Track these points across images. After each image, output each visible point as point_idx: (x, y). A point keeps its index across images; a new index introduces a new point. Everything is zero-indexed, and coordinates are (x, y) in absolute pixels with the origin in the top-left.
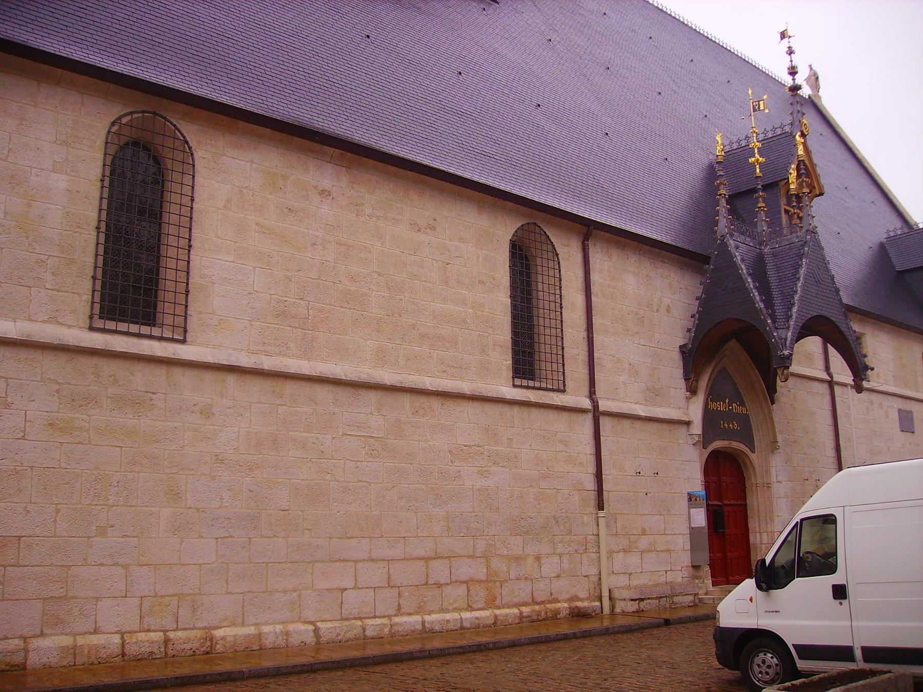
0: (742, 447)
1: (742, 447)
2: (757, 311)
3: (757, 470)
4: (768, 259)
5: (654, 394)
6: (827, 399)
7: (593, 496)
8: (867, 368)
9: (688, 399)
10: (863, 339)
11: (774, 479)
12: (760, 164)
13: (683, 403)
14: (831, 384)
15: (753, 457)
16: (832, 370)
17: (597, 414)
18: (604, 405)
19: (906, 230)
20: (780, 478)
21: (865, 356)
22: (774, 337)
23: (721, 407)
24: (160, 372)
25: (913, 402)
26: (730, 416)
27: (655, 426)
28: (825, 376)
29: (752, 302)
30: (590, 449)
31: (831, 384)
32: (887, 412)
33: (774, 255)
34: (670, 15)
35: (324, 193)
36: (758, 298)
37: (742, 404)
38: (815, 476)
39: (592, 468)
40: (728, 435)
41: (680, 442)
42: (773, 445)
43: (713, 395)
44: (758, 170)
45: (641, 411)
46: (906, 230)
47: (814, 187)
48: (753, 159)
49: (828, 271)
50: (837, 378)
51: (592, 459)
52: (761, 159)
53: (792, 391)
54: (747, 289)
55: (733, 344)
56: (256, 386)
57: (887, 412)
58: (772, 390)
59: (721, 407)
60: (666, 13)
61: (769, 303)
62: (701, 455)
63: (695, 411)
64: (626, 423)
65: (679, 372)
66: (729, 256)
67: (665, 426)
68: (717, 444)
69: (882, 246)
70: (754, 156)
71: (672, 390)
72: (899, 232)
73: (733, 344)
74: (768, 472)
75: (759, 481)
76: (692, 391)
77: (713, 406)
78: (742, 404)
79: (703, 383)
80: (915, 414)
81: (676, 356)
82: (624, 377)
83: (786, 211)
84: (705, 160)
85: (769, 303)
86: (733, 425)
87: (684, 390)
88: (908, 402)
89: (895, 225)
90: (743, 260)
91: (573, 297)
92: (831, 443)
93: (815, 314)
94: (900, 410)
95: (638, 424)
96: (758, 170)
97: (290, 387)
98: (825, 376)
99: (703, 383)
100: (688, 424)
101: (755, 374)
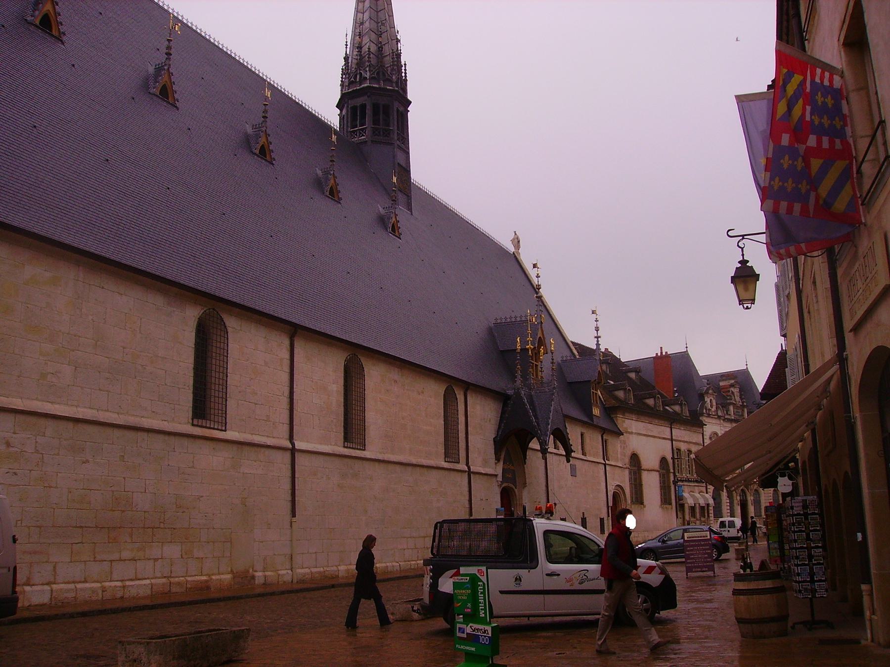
5: (485, 462)
7: (468, 510)
8: (573, 451)
15: (516, 490)
17: (470, 473)
18: (473, 469)
24: (360, 462)
30: (467, 489)
35: (396, 381)
39: (467, 498)
42: (525, 485)
51: (467, 493)
56: (383, 465)
63: (499, 470)
76: (498, 459)
91: (462, 419)
92: (544, 484)
97: (391, 467)
99: (502, 456)
100: (496, 476)
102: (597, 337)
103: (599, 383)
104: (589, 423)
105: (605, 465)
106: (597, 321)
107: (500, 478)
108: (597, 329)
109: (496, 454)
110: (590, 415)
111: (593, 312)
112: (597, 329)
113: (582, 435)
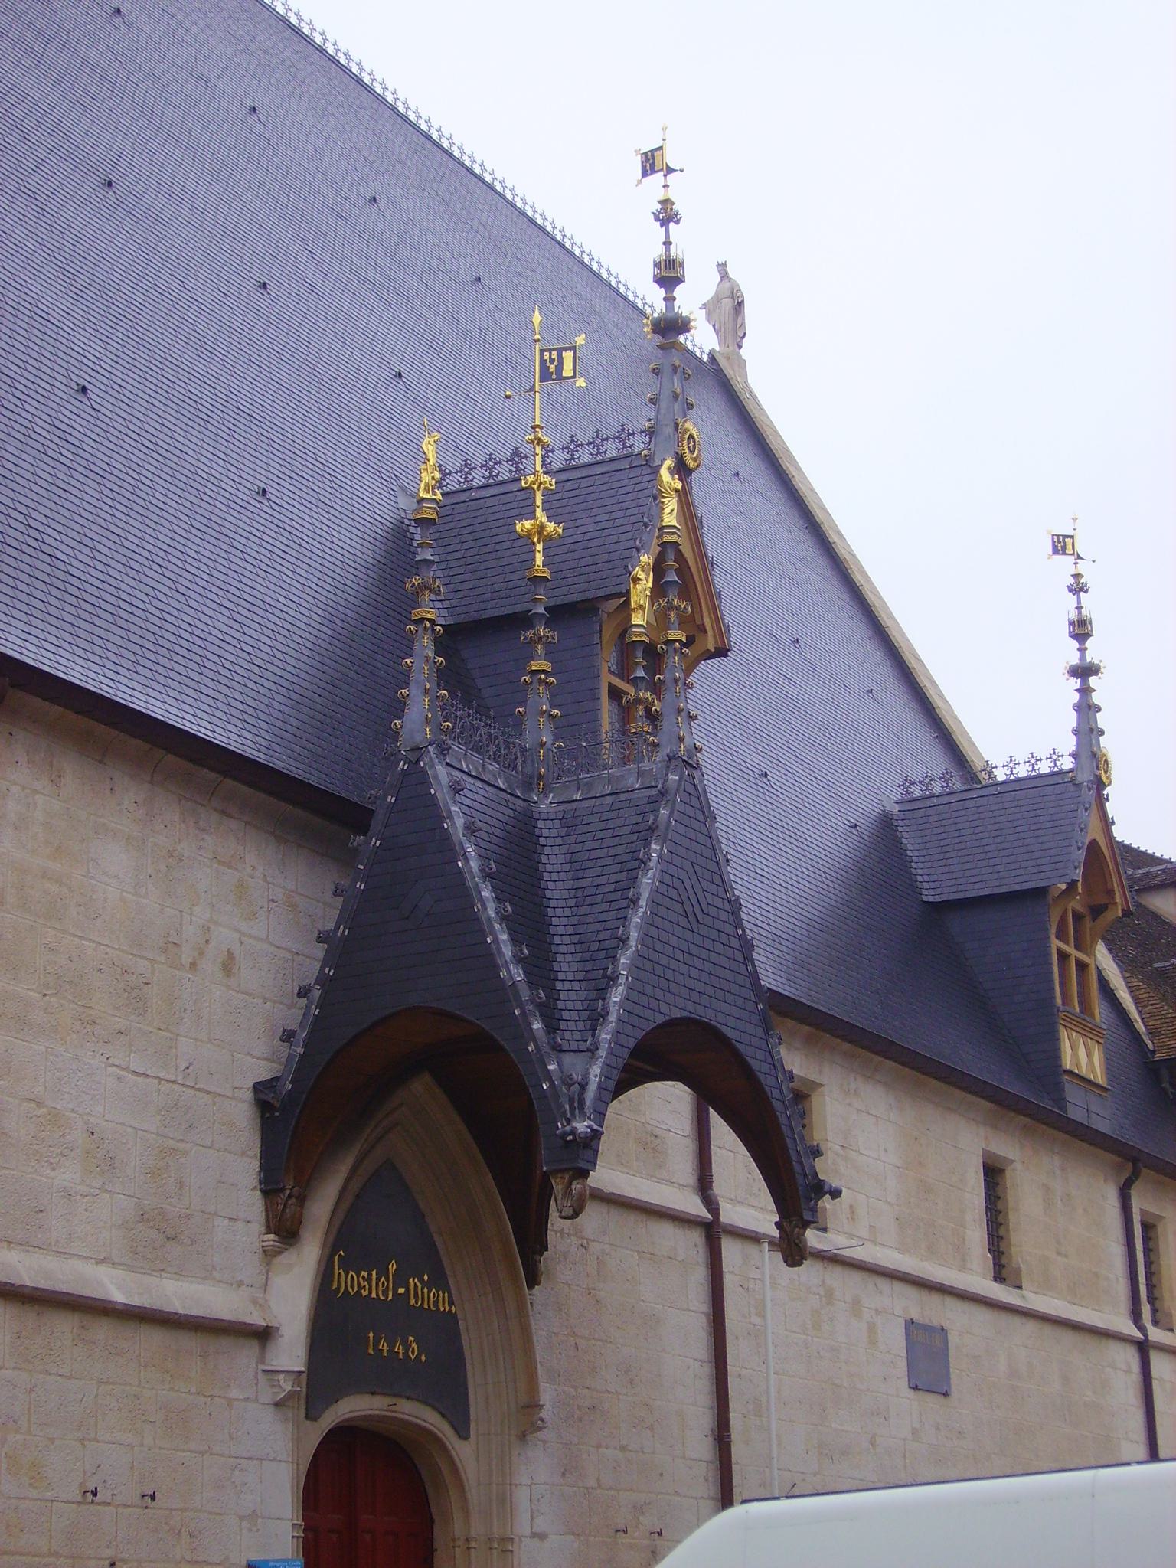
0: (430, 1418)
1: (430, 1418)
2: (504, 993)
3: (473, 1494)
4: (549, 836)
6: (699, 1275)
8: (819, 1188)
9: (269, 1255)
10: (815, 1099)
11: (522, 1525)
12: (548, 540)
13: (250, 1267)
14: (713, 1232)
15: (464, 1452)
16: (719, 1188)
19: (958, 785)
20: (541, 1524)
21: (816, 1152)
22: (548, 1076)
23: (373, 1285)
25: (951, 1302)
26: (398, 1316)
27: (154, 1339)
28: (694, 1206)
29: (489, 960)
31: (713, 1232)
32: (872, 1328)
33: (569, 823)
34: (322, 51)
36: (507, 951)
37: (439, 1280)
38: (649, 1521)
40: (388, 1377)
41: (234, 1393)
42: (527, 1418)
43: (348, 1246)
44: (539, 559)
45: (115, 1286)
46: (958, 785)
47: (703, 630)
48: (528, 524)
49: (725, 885)
50: (731, 1214)
52: (551, 526)
53: (595, 1248)
54: (477, 919)
55: (422, 1088)
57: (872, 1328)
58: (532, 1242)
59: (373, 1285)
60: (308, 40)
61: (540, 969)
62: (297, 1441)
63: (289, 1297)
64: (64, 1327)
65: (247, 1169)
66: (434, 814)
67: (188, 1342)
68: (353, 1407)
69: (886, 823)
70: (532, 515)
71: (221, 1224)
72: (937, 788)
73: (422, 1088)
74: (504, 1502)
75: (477, 1529)
76: (285, 1229)
77: (344, 1281)
78: (439, 1280)
79: (321, 1207)
80: (953, 1339)
81: (242, 1114)
82: (68, 1175)
83: (615, 694)
84: (383, 508)
85: (540, 969)
86: (407, 1346)
87: (258, 1226)
88: (935, 1299)
89: (928, 764)
90: (471, 829)
93: (677, 1014)
94: (910, 1324)
95: (103, 1331)
96: (539, 559)
98: (694, 1206)
99: (321, 1207)
100: (263, 1335)
101: (484, 1188)
102: (1084, 672)
103: (1097, 911)
104: (1030, 1098)
105: (1143, 1348)
106: (1078, 588)
107: (291, 1353)
108: (1081, 630)
109: (270, 1187)
110: (1049, 1074)
111: (1061, 545)
112: (1081, 630)
113: (993, 1173)
